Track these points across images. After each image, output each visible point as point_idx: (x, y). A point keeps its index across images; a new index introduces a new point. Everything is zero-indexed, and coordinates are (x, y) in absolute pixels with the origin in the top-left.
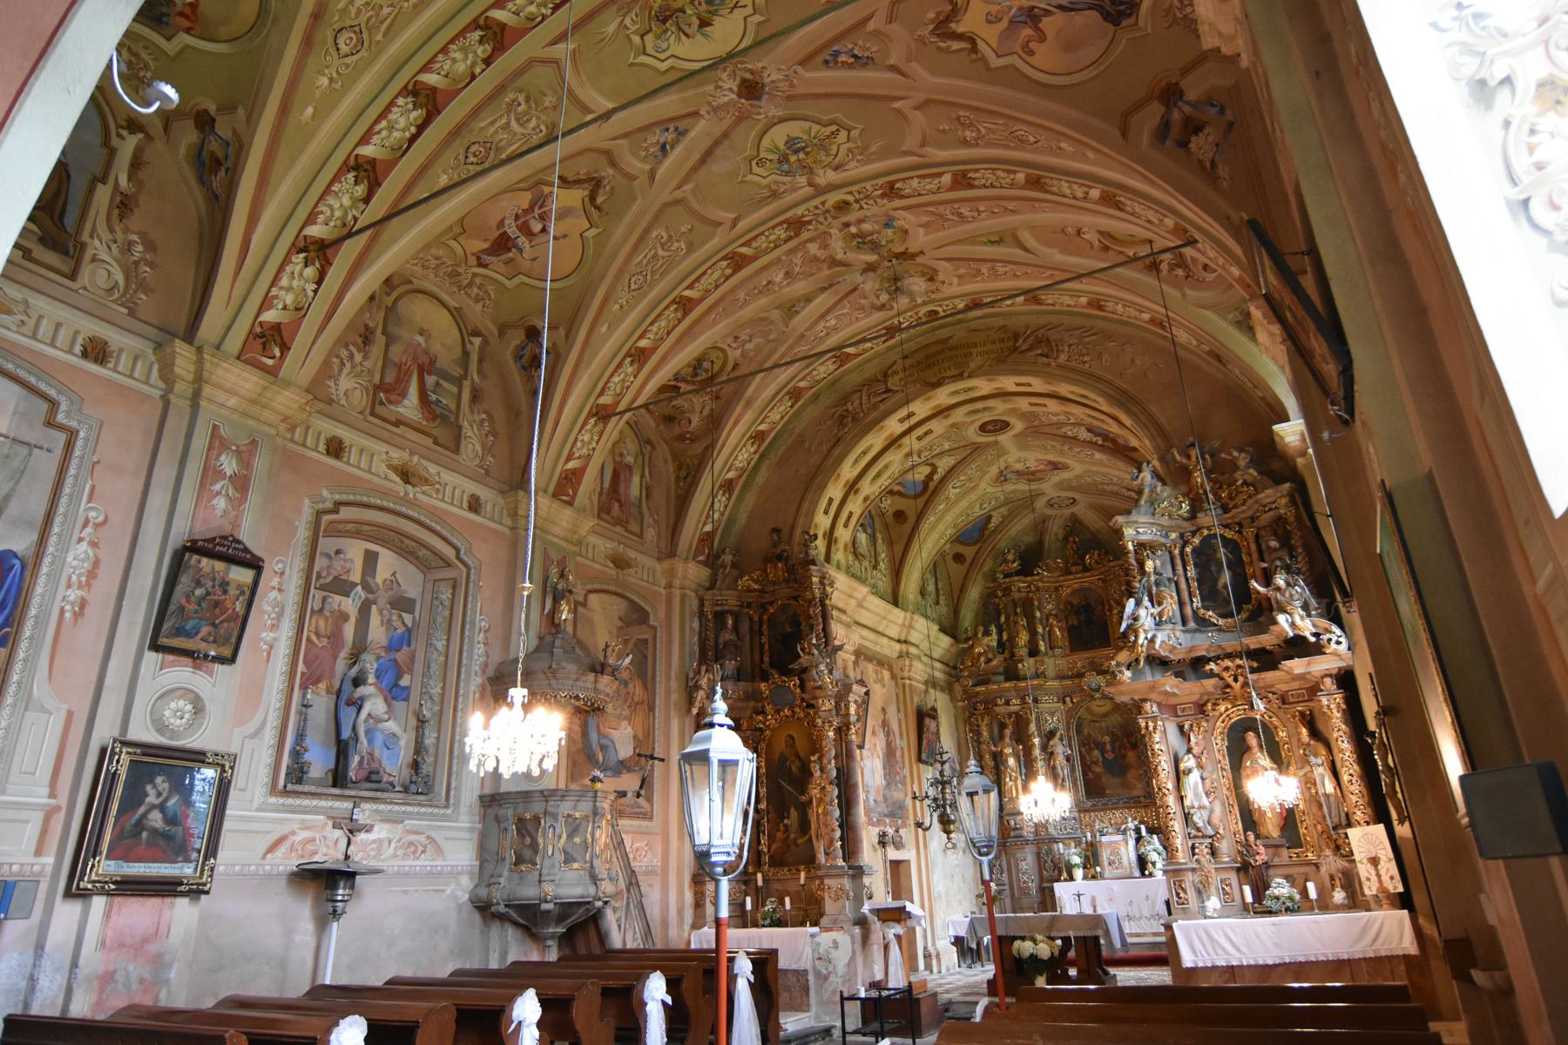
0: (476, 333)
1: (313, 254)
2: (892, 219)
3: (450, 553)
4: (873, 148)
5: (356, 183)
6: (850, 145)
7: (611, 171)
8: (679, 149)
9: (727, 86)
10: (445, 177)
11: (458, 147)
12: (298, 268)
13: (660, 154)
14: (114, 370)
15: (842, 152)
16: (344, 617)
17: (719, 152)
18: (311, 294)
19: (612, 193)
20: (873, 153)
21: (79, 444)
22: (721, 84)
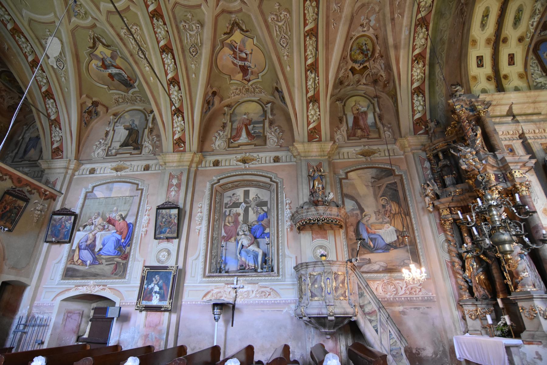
0: (268, 103)
1: (178, 113)
3: (268, 180)
5: (174, 87)
7: (233, 16)
10: (193, 65)
11: (187, 53)
12: (176, 119)
14: (151, 170)
16: (239, 215)
18: (183, 124)
19: (243, 22)
21: (144, 192)
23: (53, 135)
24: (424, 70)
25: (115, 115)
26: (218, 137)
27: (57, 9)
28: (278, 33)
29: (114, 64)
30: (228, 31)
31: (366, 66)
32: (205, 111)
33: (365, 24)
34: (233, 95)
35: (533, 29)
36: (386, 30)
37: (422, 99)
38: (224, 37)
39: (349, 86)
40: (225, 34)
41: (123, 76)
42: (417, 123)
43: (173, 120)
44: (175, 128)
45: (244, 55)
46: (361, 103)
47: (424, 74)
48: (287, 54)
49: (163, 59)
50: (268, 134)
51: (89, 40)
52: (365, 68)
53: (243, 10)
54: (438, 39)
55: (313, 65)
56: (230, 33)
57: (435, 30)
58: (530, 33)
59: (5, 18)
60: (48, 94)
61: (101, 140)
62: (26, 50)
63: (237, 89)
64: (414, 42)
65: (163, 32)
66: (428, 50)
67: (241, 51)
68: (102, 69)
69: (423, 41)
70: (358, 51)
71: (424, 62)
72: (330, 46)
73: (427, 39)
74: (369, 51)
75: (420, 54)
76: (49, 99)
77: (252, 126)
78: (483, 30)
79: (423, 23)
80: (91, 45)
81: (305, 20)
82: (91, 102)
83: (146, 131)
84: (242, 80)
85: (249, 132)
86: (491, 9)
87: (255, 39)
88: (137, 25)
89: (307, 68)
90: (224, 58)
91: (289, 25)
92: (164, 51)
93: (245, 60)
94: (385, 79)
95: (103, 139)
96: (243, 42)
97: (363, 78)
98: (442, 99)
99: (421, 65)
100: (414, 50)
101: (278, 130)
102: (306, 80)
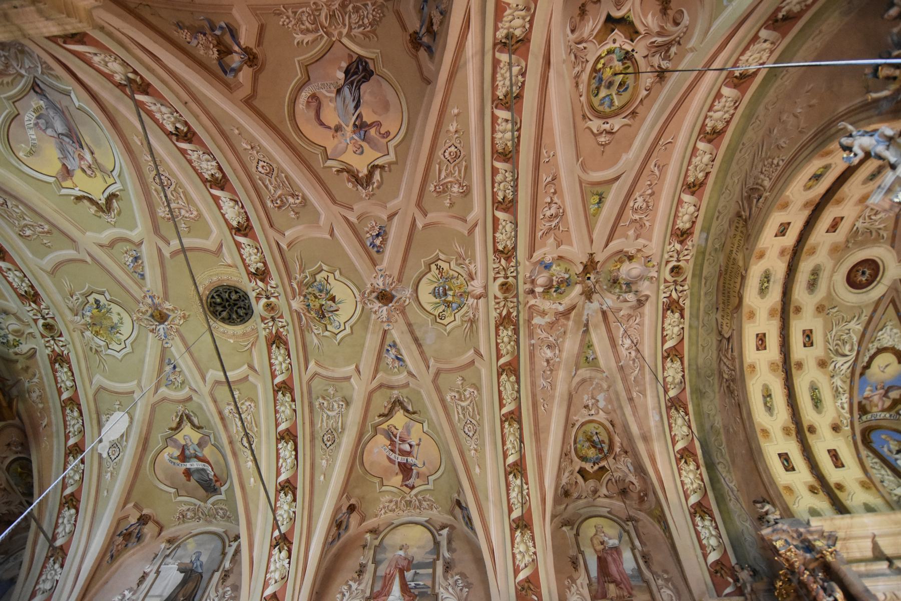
0: (443, 528)
2: (541, 262)
4: (461, 251)
5: (286, 495)
6: (453, 264)
7: (396, 392)
8: (403, 352)
9: (377, 308)
10: (324, 461)
11: (319, 443)
12: (277, 557)
13: (401, 363)
15: (459, 270)
17: (418, 334)
20: (466, 253)
22: (374, 310)
23: (44, 577)
24: (701, 474)
25: (170, 541)
26: (347, 595)
27: (144, 376)
28: (461, 416)
29: (199, 454)
30: (386, 412)
31: (604, 467)
32: (330, 540)
33: (590, 406)
34: (383, 511)
35: (847, 413)
36: (624, 414)
37: (712, 525)
38: (378, 420)
39: (580, 499)
40: (380, 416)
41: (208, 474)
42: (717, 572)
43: (270, 555)
44: (272, 572)
45: (406, 447)
46: (606, 530)
47: (702, 480)
48: (475, 447)
49: (278, 450)
50: (441, 589)
51: (174, 418)
52: (603, 469)
53: (411, 385)
54: (707, 426)
55: (517, 465)
56: (388, 415)
57: (699, 414)
58: (846, 419)
59: (65, 384)
60: (72, 501)
61: (126, 592)
62: (72, 429)
63: (391, 501)
64: (671, 431)
65: (288, 412)
66: (697, 444)
67: (403, 441)
68: (178, 461)
69: (685, 429)
70: (587, 444)
71: (696, 461)
72: (542, 436)
73: (690, 427)
74: (604, 443)
75: (685, 449)
76: (69, 509)
77: (412, 571)
78: (771, 415)
79: (676, 404)
80: (174, 425)
81: (501, 399)
82: (138, 515)
83: (217, 575)
84: (402, 486)
85: (407, 585)
86: (771, 387)
87: (425, 425)
88: (252, 400)
89: (509, 469)
90: (376, 450)
91: (477, 406)
92: (282, 438)
93: (409, 454)
94: (638, 488)
95: (130, 590)
96: (408, 429)
97: (601, 485)
98: (747, 524)
99: (692, 466)
100: (674, 443)
101: (460, 581)
102: (508, 490)
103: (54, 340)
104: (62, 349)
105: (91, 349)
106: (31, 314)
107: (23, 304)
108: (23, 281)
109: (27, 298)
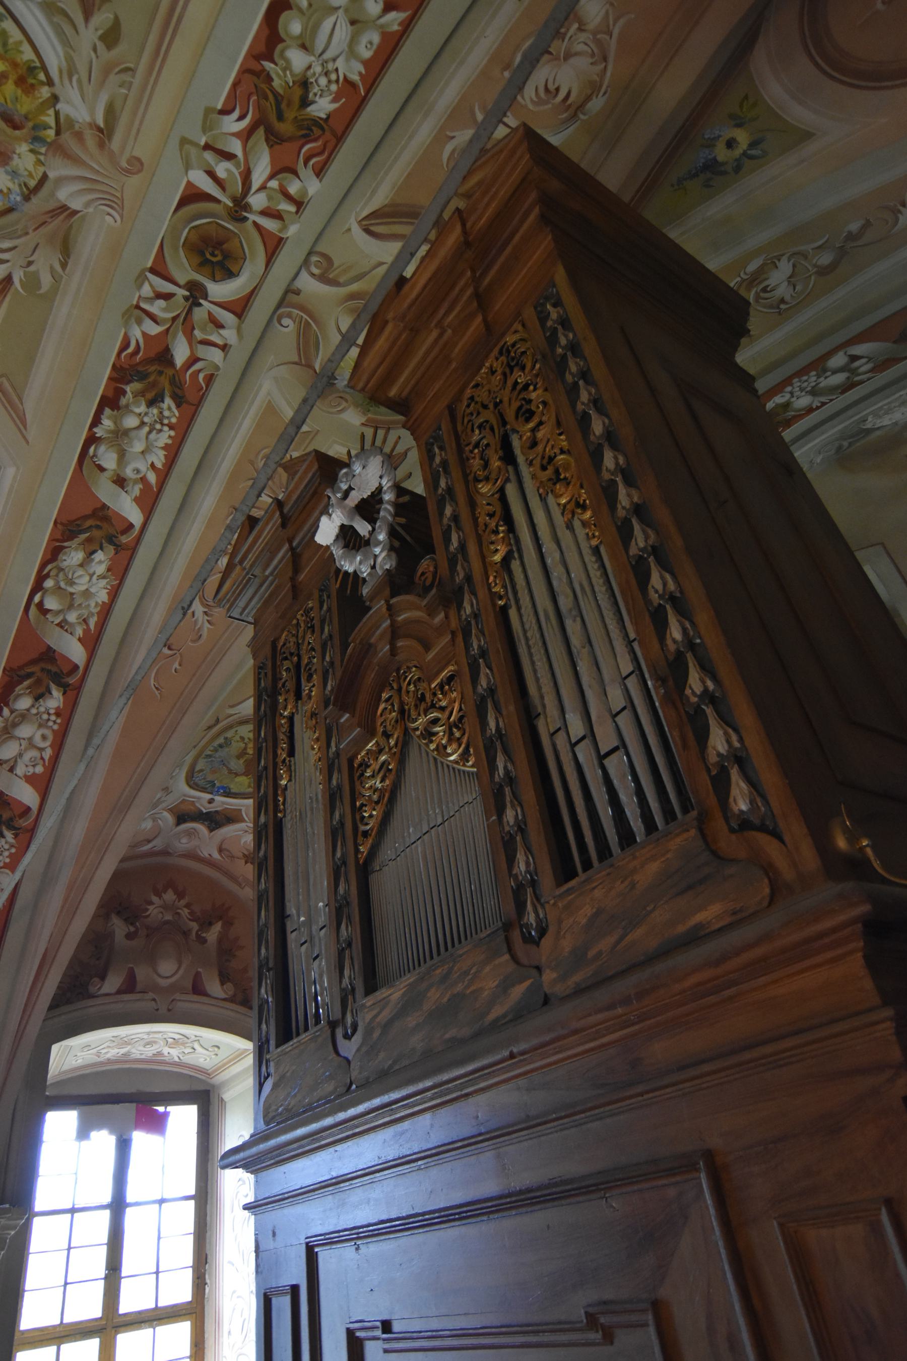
103: (240, 207)
104: (236, 147)
105: (111, 37)
106: (229, 335)
107: (210, 379)
108: (120, 435)
109: (176, 384)
